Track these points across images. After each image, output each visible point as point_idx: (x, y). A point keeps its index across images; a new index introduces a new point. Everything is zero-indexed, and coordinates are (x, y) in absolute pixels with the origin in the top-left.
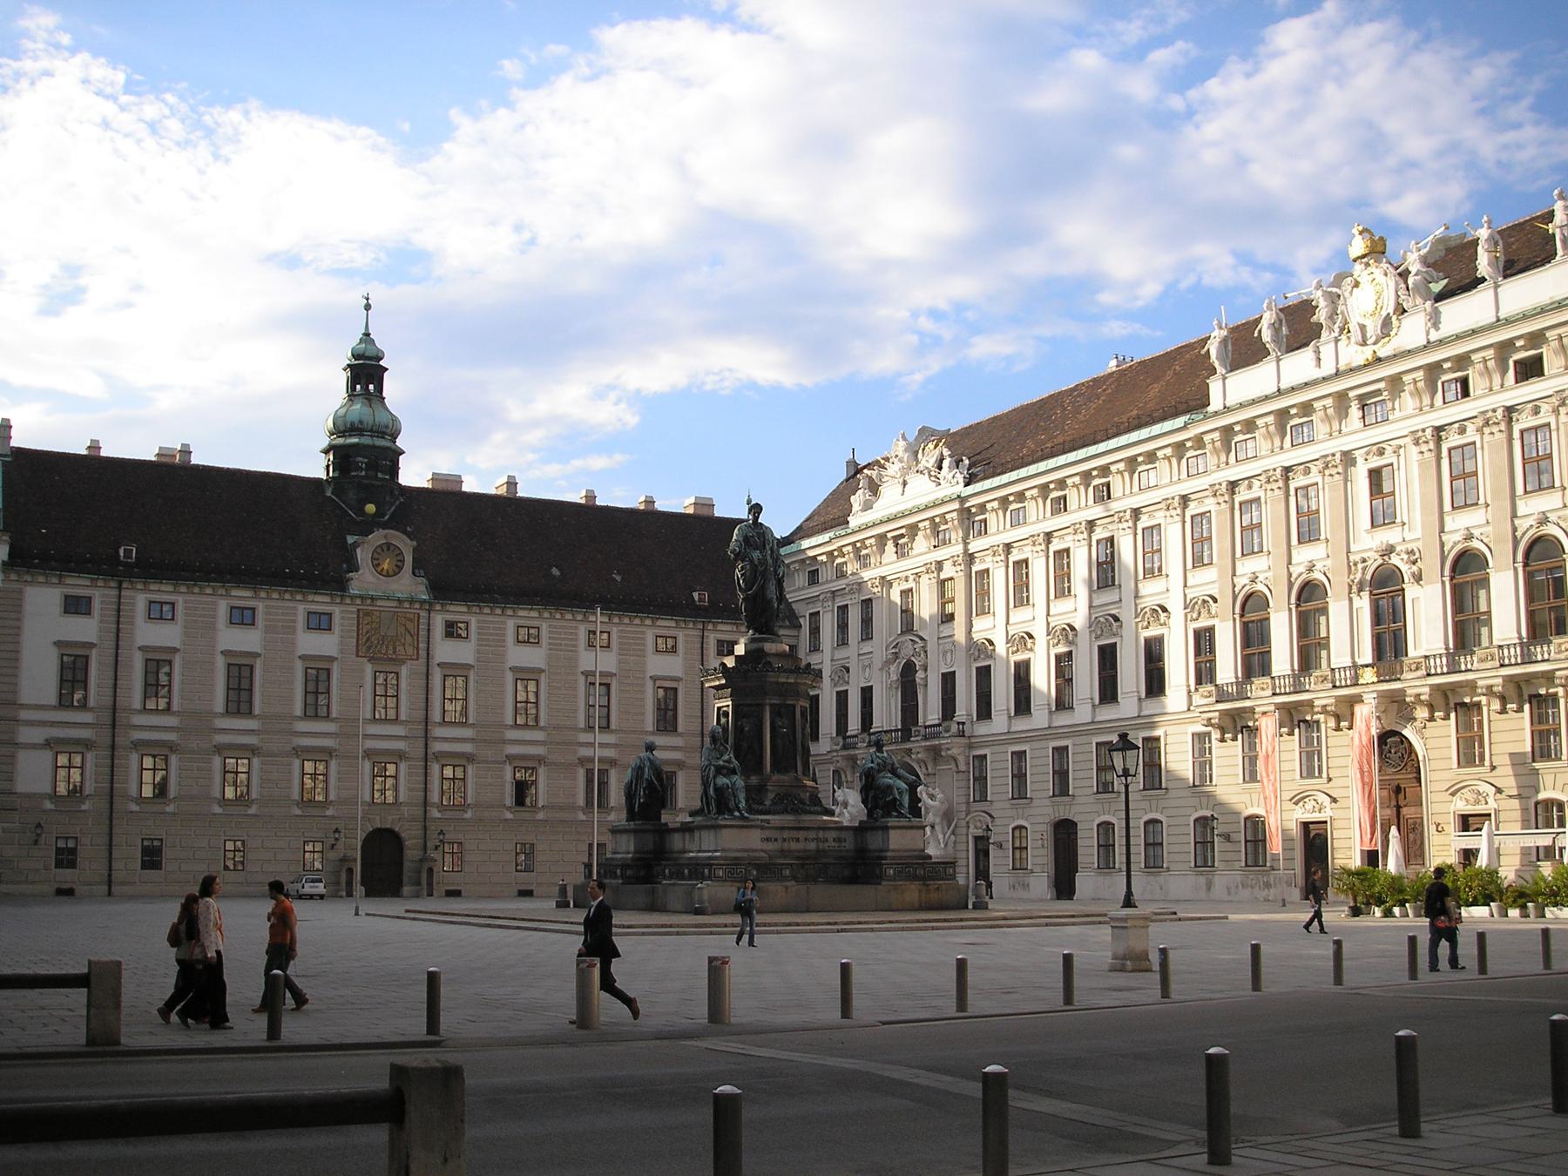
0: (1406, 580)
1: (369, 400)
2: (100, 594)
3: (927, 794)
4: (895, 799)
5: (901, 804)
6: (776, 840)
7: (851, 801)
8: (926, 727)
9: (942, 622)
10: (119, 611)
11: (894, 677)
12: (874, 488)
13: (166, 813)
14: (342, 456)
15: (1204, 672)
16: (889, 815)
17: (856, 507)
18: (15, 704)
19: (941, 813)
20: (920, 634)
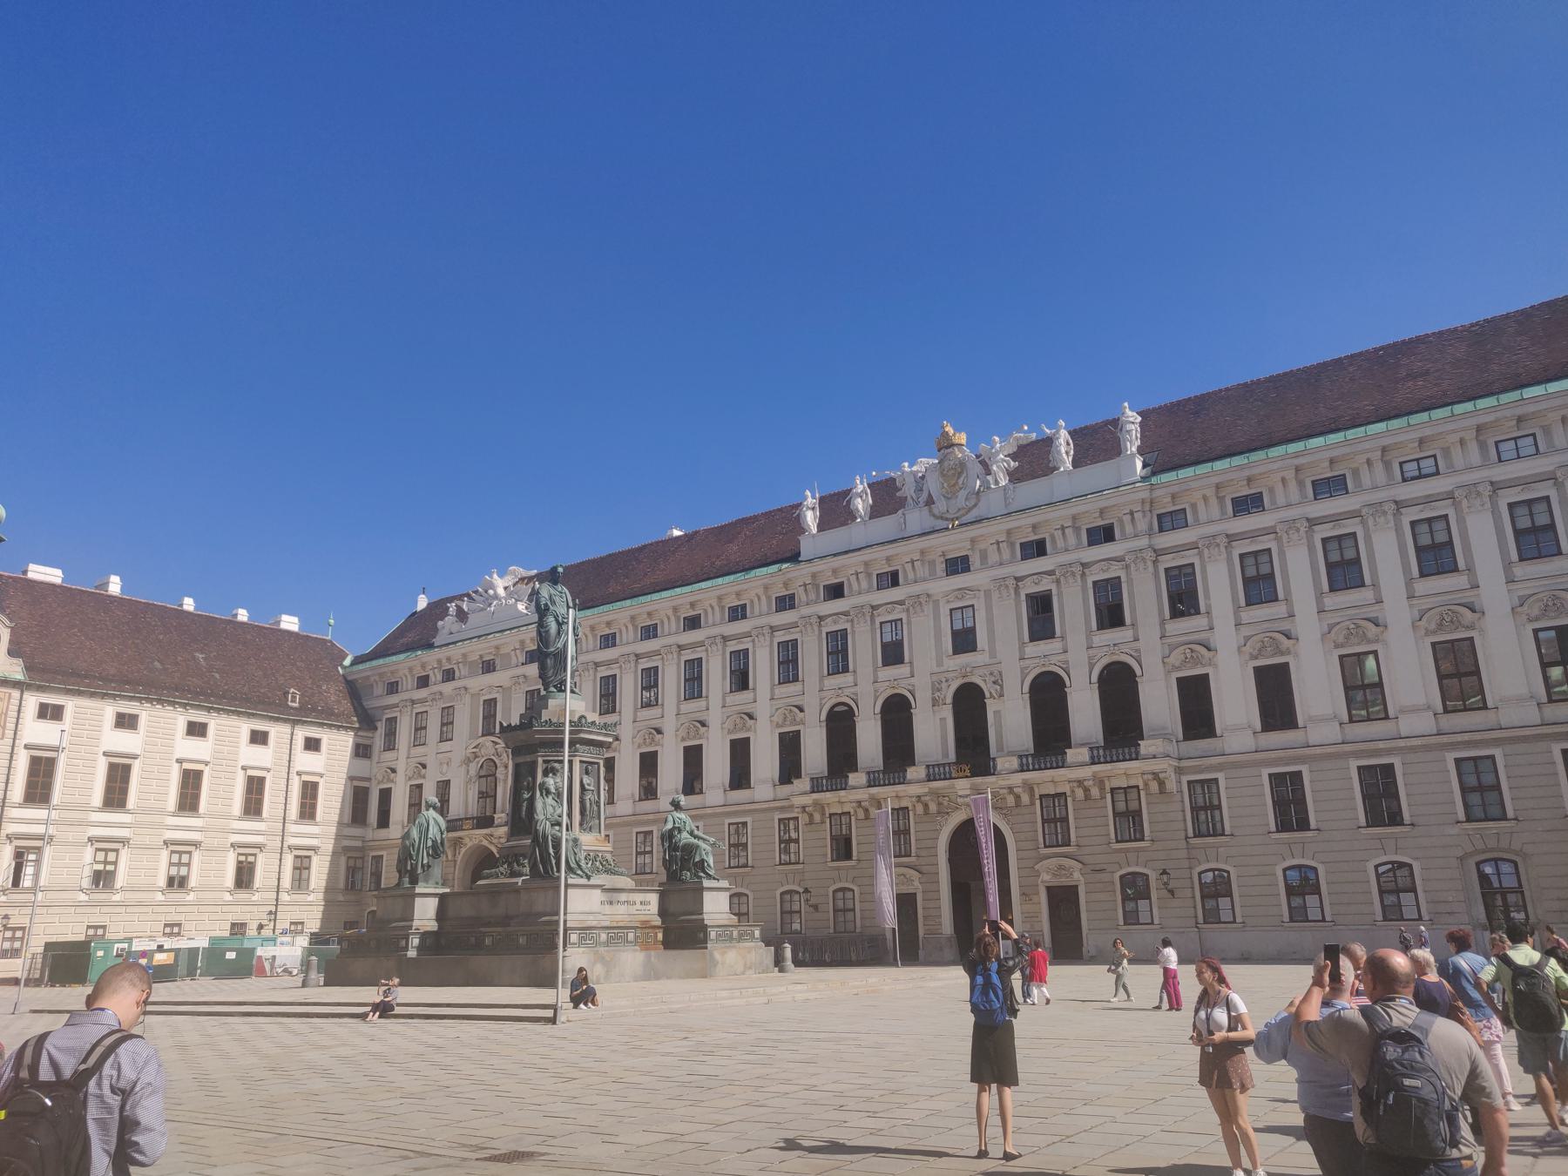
0: (987, 695)
11: (473, 772)
12: (462, 616)
15: (790, 767)
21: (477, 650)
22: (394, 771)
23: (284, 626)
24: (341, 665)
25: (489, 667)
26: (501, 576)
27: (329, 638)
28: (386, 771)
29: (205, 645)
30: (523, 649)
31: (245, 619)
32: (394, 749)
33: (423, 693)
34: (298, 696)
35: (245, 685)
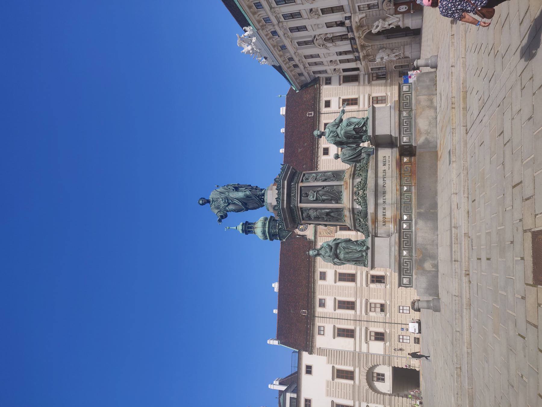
1: (255, 228)
2: (318, 323)
3: (376, 29)
4: (354, 129)
5: (357, 124)
6: (384, 209)
7: (381, 56)
8: (349, 32)
9: (307, 30)
10: (323, 317)
11: (331, 45)
13: (389, 305)
14: (273, 237)
16: (366, 131)
17: (273, 64)
18: (354, 353)
19: (384, 22)
20: (313, 37)
21: (276, 53)
22: (335, 69)
23: (284, 113)
24: (296, 91)
25: (283, 48)
26: (243, 49)
27: (286, 96)
28: (336, 72)
29: (295, 148)
30: (272, 37)
31: (284, 129)
32: (326, 70)
33: (301, 66)
34: (309, 113)
35: (308, 134)
